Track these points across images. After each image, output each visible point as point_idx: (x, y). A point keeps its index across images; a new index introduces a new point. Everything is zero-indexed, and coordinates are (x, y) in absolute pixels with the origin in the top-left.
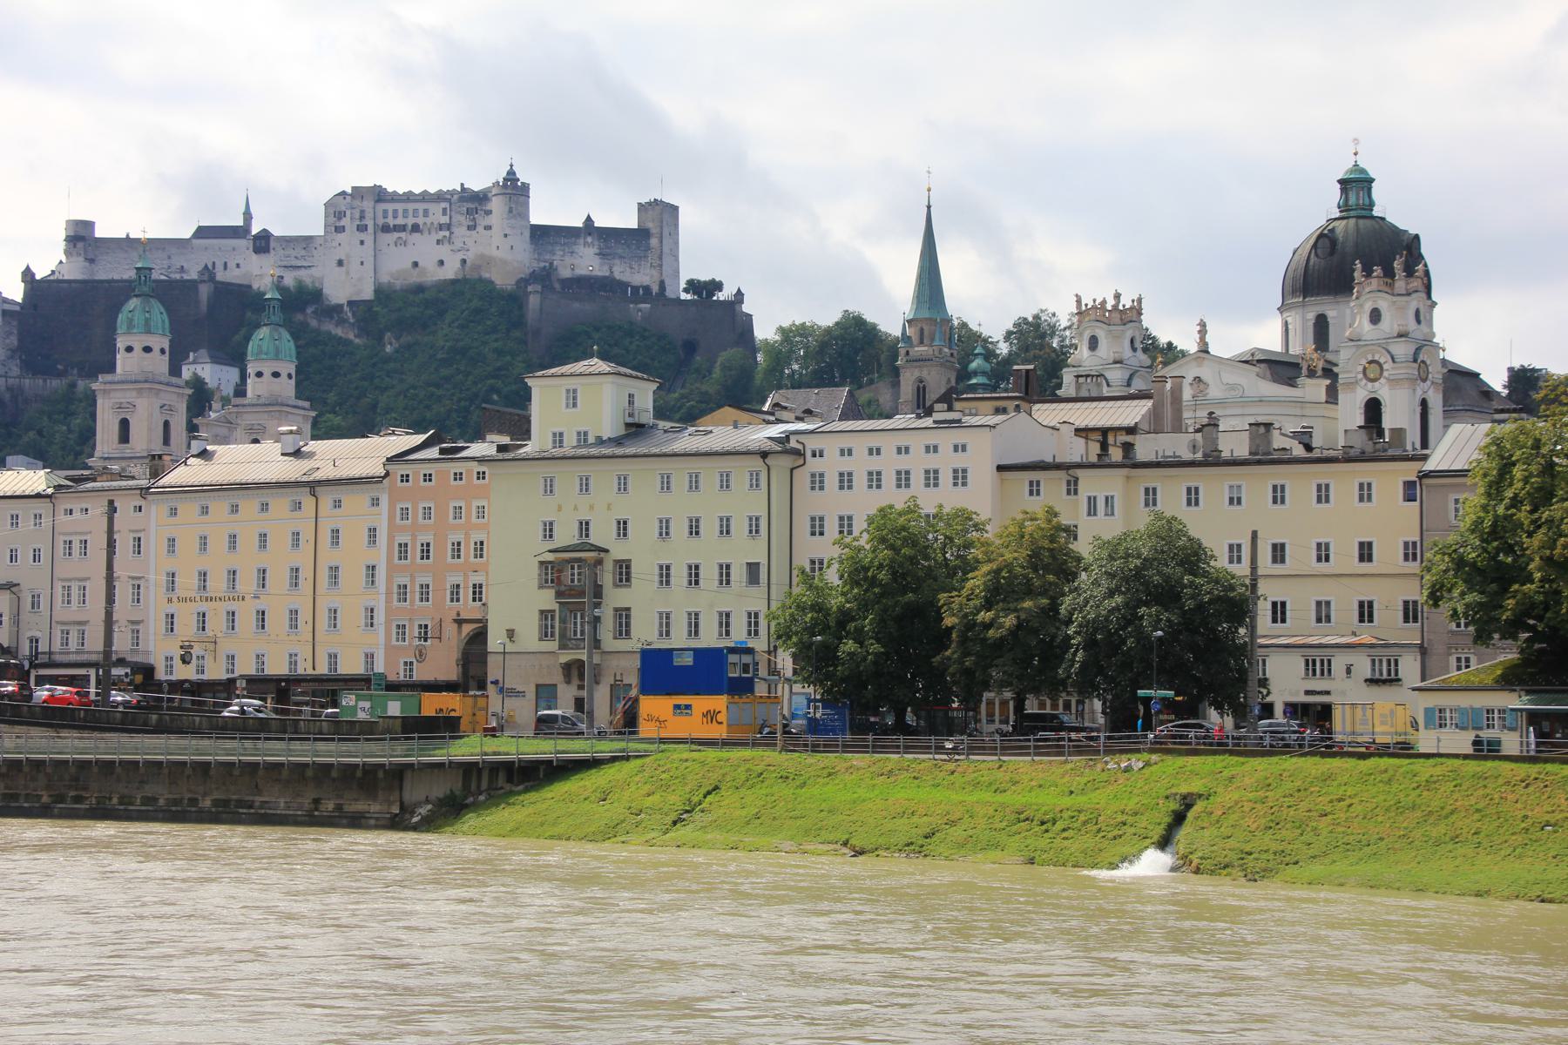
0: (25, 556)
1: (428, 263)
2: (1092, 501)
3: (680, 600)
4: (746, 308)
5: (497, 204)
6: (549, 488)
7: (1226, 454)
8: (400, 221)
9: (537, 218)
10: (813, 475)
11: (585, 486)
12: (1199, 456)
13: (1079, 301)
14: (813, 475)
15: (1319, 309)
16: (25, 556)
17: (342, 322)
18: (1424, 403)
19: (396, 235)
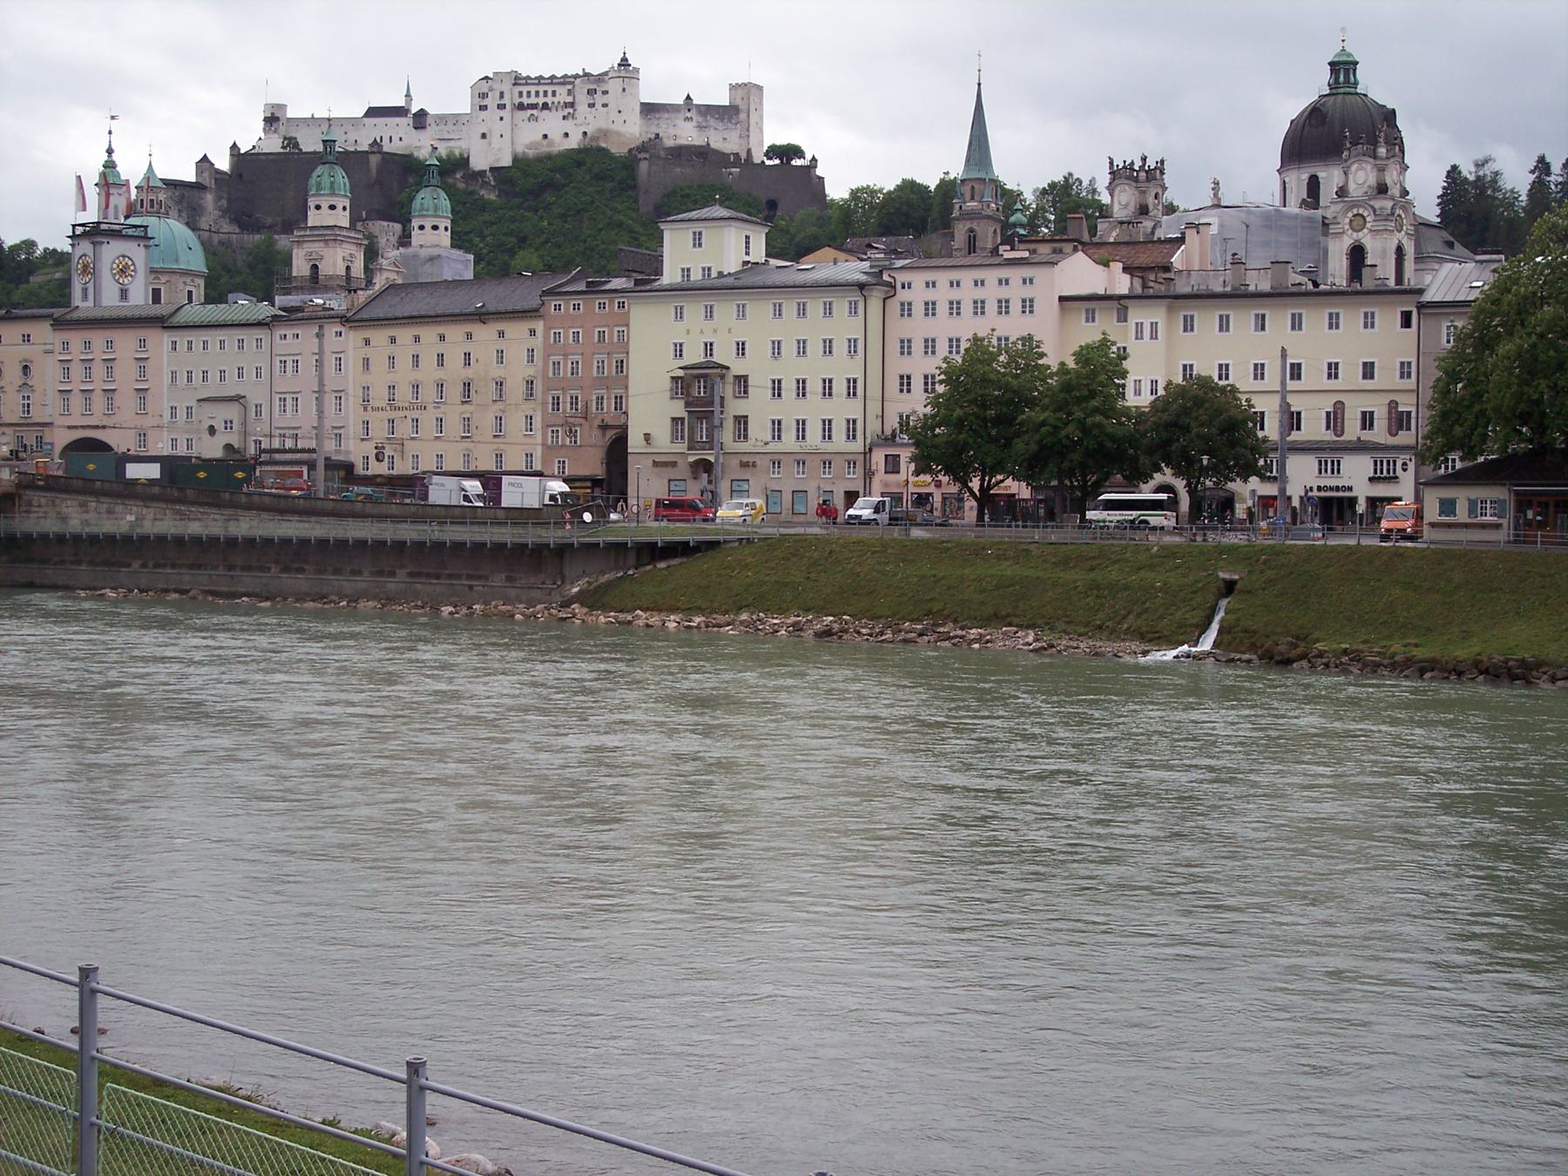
0: (250, 374)
1: (555, 136)
2: (1139, 326)
3: (789, 409)
4: (819, 172)
5: (614, 86)
6: (679, 314)
7: (1252, 288)
8: (533, 100)
10: (902, 304)
11: (709, 314)
12: (1228, 289)
13: (1111, 163)
14: (902, 304)
15: (1313, 171)
16: (250, 374)
17: (485, 184)
18: (1400, 251)
19: (530, 112)
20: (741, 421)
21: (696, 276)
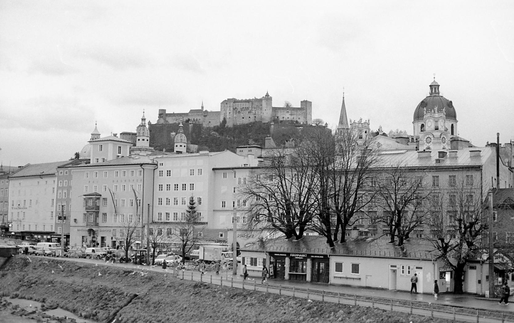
5: (264, 103)
9: (274, 106)
20: (105, 214)
21: (100, 161)
